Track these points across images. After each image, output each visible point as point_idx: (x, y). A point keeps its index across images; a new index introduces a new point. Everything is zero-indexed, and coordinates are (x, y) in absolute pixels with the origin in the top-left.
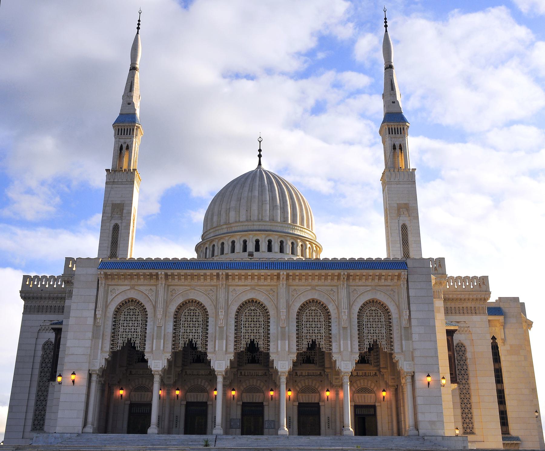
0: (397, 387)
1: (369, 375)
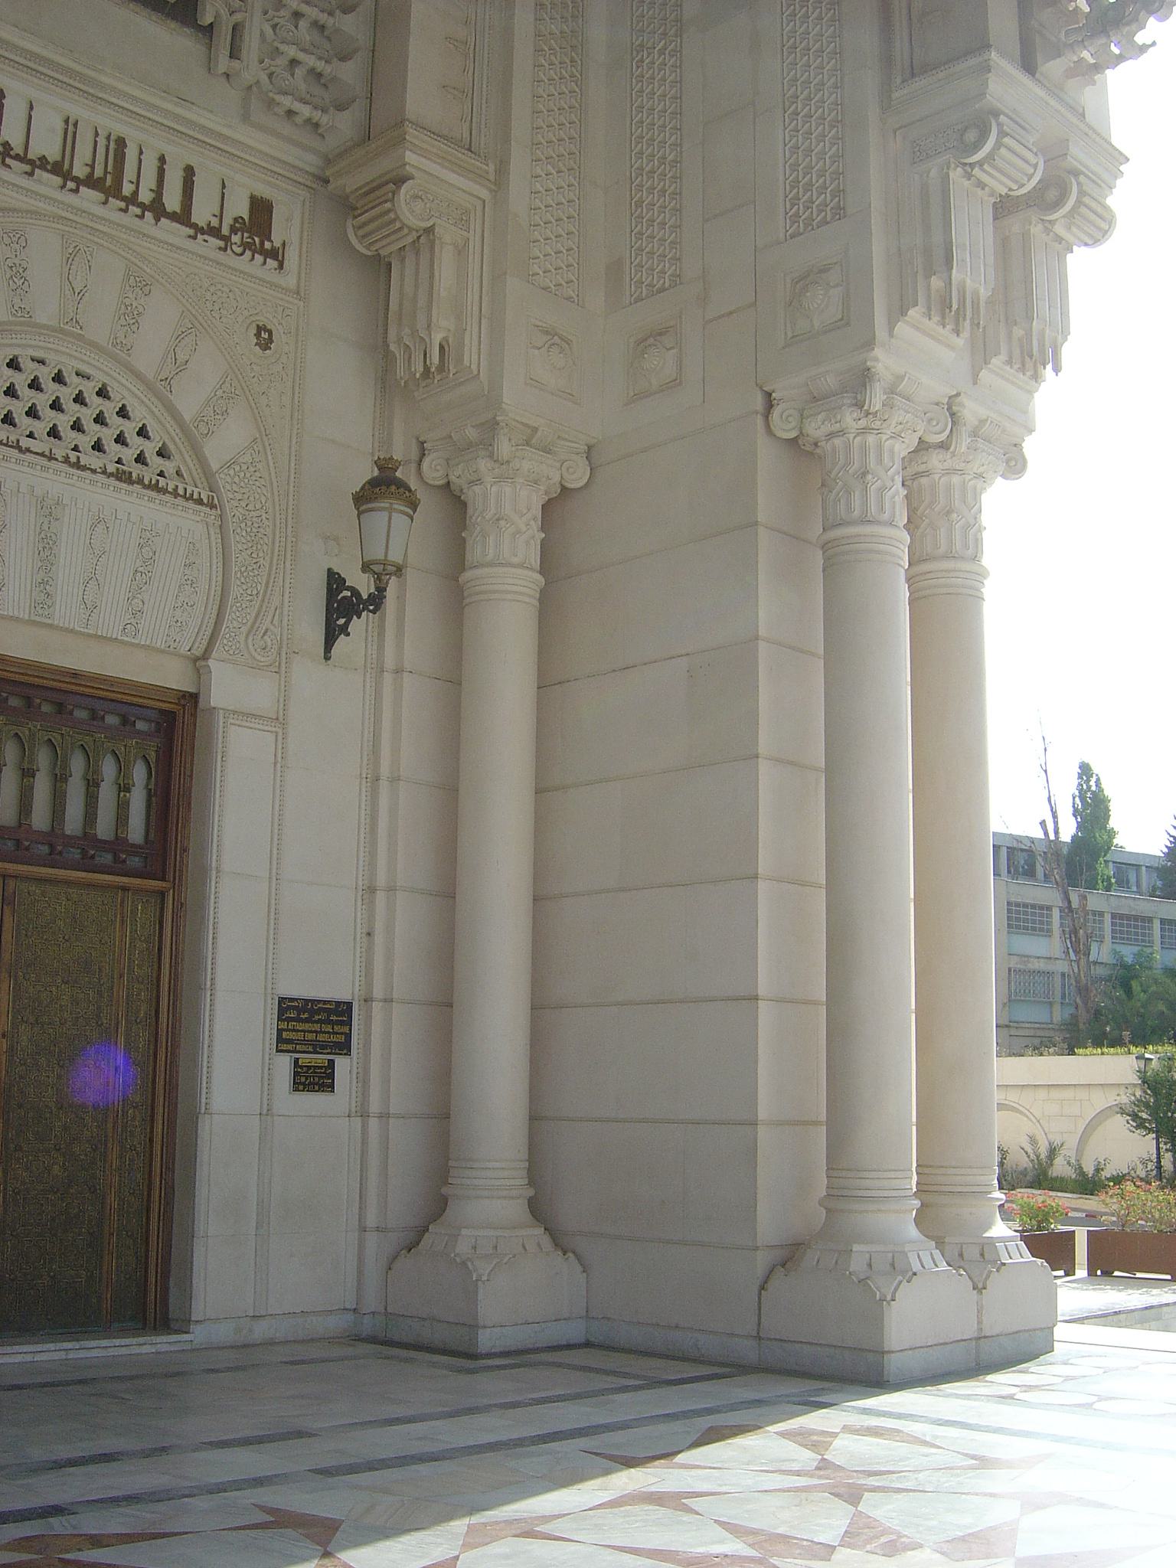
0: (578, 477)
1: (172, 201)
